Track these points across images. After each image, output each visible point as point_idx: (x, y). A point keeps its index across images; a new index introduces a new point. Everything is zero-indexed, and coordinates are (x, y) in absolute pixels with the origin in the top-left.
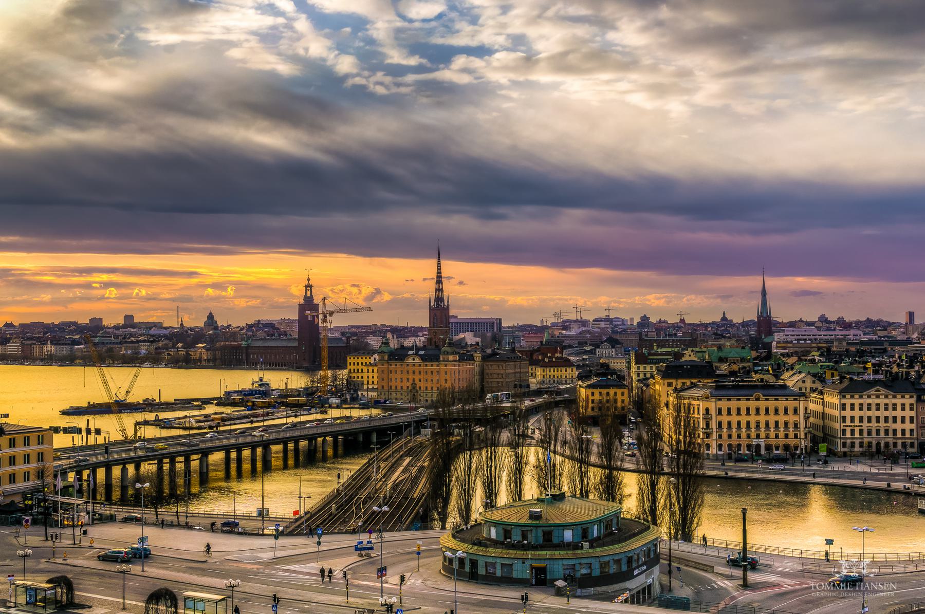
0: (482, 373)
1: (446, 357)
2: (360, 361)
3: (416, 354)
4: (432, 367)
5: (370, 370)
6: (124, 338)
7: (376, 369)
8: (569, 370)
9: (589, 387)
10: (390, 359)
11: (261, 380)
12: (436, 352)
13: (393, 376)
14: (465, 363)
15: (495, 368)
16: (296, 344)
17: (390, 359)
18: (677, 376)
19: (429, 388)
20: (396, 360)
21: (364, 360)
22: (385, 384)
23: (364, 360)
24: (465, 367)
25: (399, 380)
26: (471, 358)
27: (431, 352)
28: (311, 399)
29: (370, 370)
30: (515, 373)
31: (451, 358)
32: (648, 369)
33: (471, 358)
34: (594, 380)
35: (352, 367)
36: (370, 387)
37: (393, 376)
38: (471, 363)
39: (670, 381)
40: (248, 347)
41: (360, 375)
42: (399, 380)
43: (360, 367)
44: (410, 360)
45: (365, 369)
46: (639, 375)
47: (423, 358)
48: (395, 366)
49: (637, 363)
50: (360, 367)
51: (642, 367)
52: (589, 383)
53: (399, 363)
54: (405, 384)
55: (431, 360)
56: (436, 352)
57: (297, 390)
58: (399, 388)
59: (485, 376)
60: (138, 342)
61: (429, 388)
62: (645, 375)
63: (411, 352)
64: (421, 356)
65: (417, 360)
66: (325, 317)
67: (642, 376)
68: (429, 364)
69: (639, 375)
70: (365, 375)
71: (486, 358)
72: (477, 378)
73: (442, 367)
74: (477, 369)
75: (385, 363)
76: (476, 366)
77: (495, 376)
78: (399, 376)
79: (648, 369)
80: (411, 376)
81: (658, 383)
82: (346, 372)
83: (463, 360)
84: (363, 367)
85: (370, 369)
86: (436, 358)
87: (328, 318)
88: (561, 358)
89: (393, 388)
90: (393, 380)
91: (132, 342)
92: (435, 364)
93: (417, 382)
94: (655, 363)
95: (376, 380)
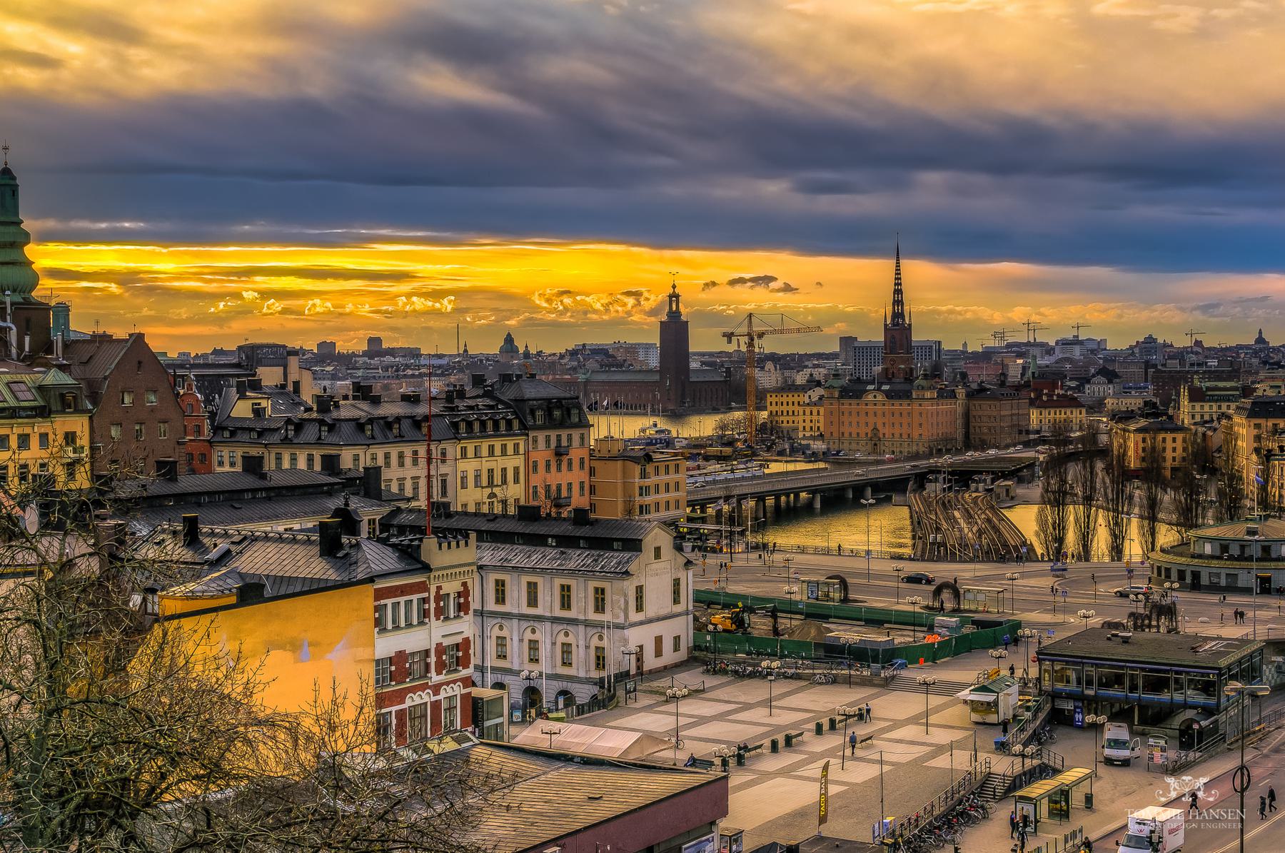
0: (967, 416)
1: (920, 393)
2: (785, 399)
3: (879, 389)
4: (901, 406)
5: (808, 412)
6: (397, 371)
7: (822, 410)
8: (1076, 412)
9: (1138, 430)
10: (841, 397)
11: (655, 425)
12: (906, 387)
13: (846, 419)
14: (945, 401)
15: (984, 409)
16: (657, 377)
17: (841, 397)
18: (1267, 415)
19: (897, 435)
20: (850, 397)
21: (796, 399)
22: (834, 429)
23: (796, 399)
24: (945, 406)
25: (854, 424)
26: (953, 395)
27: (899, 387)
28: (723, 449)
29: (808, 412)
30: (1012, 415)
31: (928, 395)
32: (1207, 408)
33: (953, 395)
34: (1143, 423)
35: (774, 408)
36: (808, 434)
37: (846, 419)
38: (953, 401)
39: (1258, 421)
40: (587, 382)
41: (791, 419)
42: (854, 424)
43: (785, 408)
44: (870, 397)
45: (801, 409)
46: (1193, 417)
47: (888, 395)
48: (849, 405)
49: (1191, 400)
50: (790, 408)
51: (1198, 405)
52: (1138, 426)
53: (854, 401)
54: (863, 430)
55: (900, 398)
56: (906, 387)
57: (709, 438)
58: (854, 435)
59: (972, 419)
60: (421, 375)
61: (897, 435)
62: (1202, 416)
63: (870, 387)
64: (883, 391)
65: (880, 397)
66: (752, 339)
67: (1198, 419)
68: (897, 402)
69: (1193, 417)
70: (801, 418)
71: (971, 395)
72: (960, 422)
73: (916, 407)
74: (960, 410)
75: (835, 402)
76: (958, 406)
77: (984, 419)
78: (854, 419)
79: (1207, 408)
80: (871, 420)
81: (1239, 425)
82: (765, 414)
83: (942, 397)
84: (796, 408)
85: (808, 410)
86: (906, 395)
87: (756, 341)
88: (1064, 396)
89: (846, 435)
90: (846, 423)
91: (413, 376)
92: (906, 402)
93: (879, 427)
94: (1216, 401)
95: (821, 425)
